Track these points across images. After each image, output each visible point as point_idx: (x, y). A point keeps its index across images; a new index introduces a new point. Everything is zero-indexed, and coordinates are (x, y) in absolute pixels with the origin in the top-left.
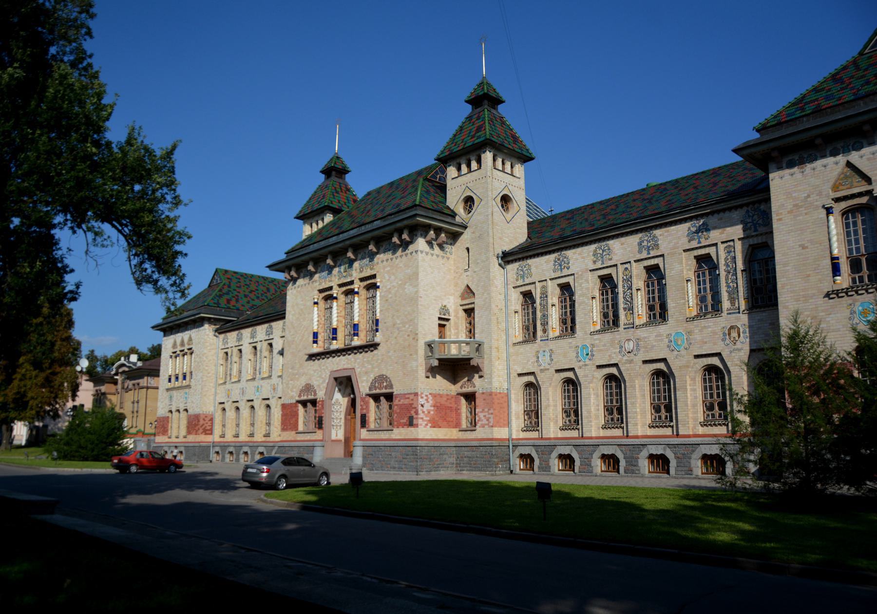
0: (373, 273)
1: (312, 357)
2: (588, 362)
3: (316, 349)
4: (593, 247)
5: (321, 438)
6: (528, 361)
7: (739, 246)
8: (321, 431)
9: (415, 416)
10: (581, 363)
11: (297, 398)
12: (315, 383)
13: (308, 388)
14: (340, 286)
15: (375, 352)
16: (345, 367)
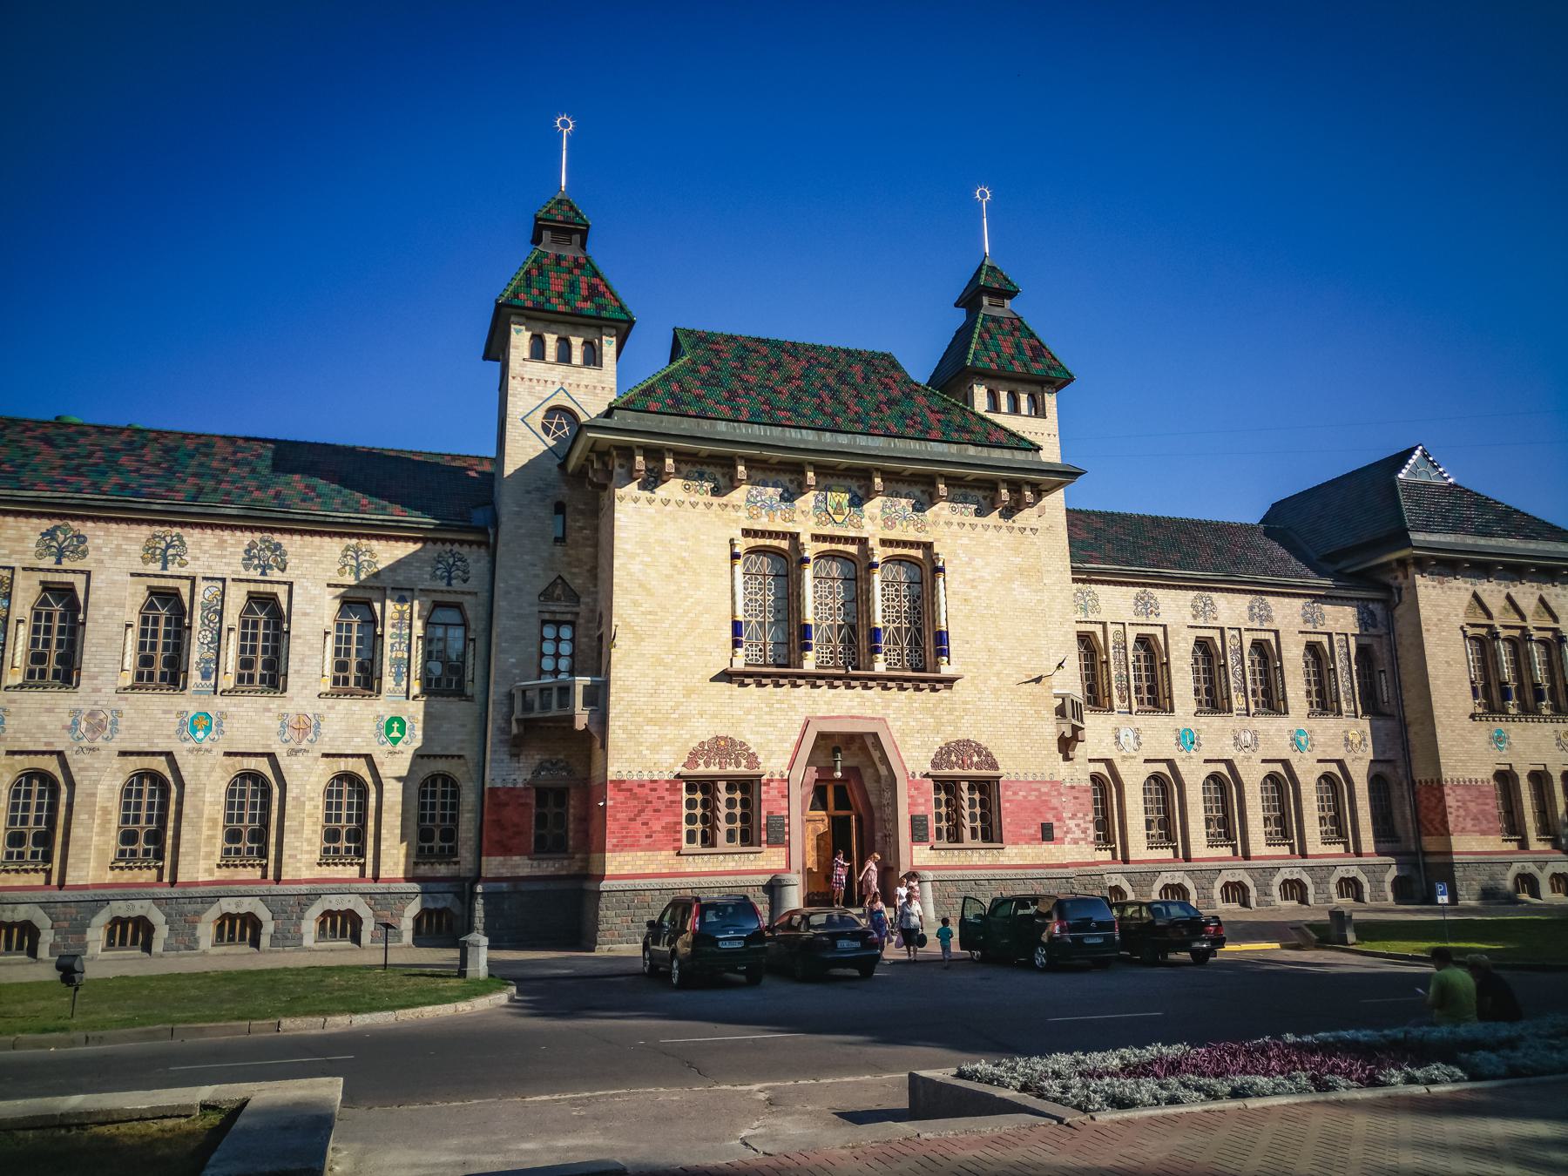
0: (923, 538)
1: (726, 676)
2: (1193, 753)
3: (739, 664)
4: (1192, 594)
5: (782, 864)
6: (1101, 741)
7: (1352, 641)
8: (783, 850)
9: (1056, 824)
10: (1184, 754)
11: (679, 769)
12: (753, 741)
13: (724, 747)
14: (816, 538)
15: (944, 693)
16: (855, 712)
